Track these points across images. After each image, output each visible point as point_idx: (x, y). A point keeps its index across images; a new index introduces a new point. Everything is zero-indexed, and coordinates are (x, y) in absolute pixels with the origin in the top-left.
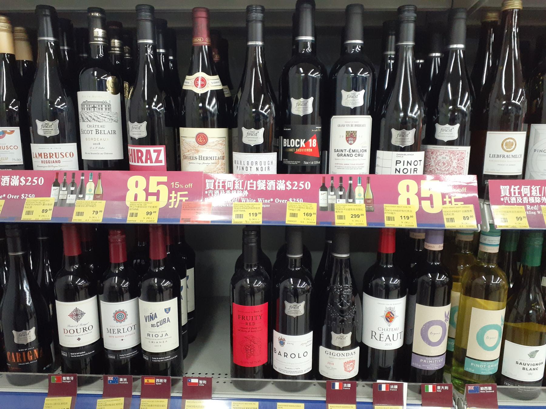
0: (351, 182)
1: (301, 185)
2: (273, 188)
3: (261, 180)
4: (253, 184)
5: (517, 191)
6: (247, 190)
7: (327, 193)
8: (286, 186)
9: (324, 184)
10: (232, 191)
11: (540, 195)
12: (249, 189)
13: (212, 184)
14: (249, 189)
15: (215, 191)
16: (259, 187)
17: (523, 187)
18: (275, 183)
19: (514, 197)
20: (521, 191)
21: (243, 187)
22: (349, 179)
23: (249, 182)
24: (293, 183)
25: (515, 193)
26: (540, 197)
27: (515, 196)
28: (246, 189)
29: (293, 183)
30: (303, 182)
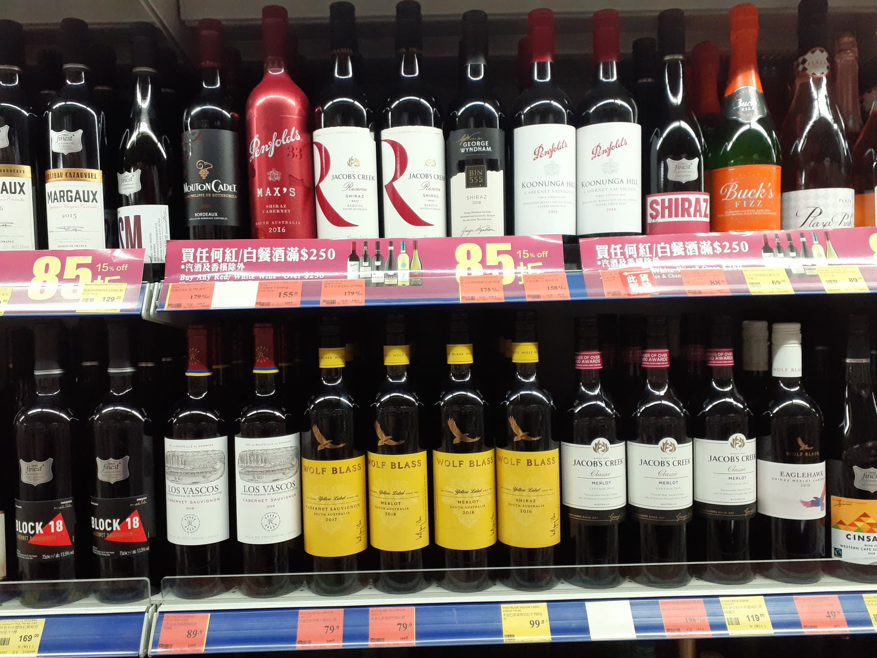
0: (392, 248)
1: (321, 253)
2: (281, 259)
3: (264, 248)
4: (252, 253)
5: (619, 251)
6: (243, 262)
7: (358, 265)
8: (301, 255)
9: (354, 252)
10: (221, 265)
11: (651, 256)
12: (245, 260)
13: (192, 255)
14: (245, 260)
15: (195, 264)
16: (261, 258)
17: (627, 245)
18: (283, 251)
19: (615, 259)
20: (625, 250)
21: (237, 258)
22: (389, 245)
23: (246, 251)
24: (311, 251)
25: (616, 254)
27: (616, 257)
28: (242, 260)
29: (311, 251)
30: (324, 250)
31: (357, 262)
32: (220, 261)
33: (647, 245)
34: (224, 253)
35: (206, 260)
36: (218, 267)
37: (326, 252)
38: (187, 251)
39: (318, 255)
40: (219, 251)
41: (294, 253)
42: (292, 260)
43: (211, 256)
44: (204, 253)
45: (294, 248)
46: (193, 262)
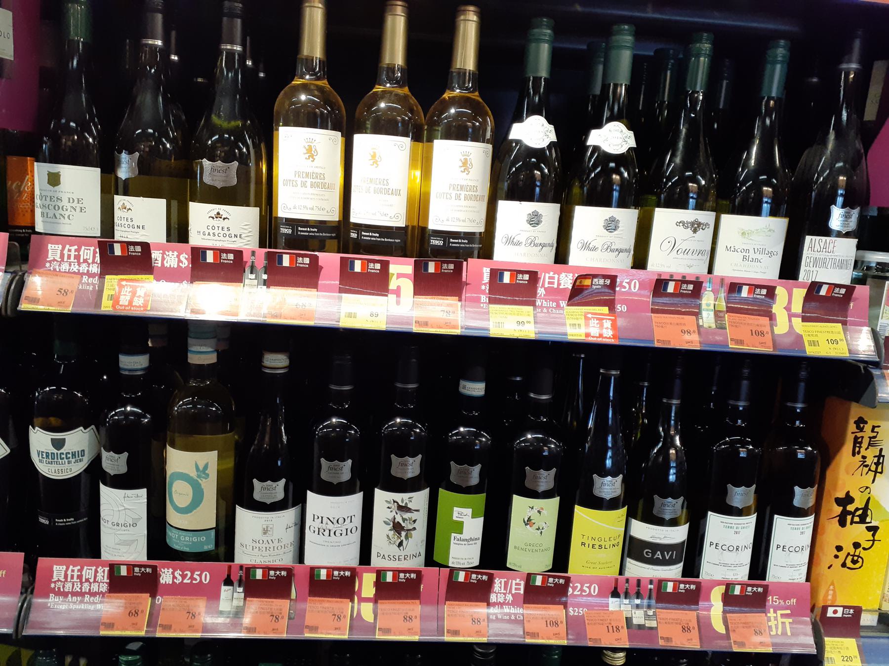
1: (195, 576)
7: (232, 589)
8: (174, 577)
9: (229, 576)
10: (92, 585)
11: (505, 592)
15: (66, 583)
24: (185, 573)
26: (505, 594)
29: (185, 573)
30: (198, 573)
31: (231, 587)
32: (92, 580)
33: (503, 580)
34: (96, 572)
35: (77, 579)
36: (89, 587)
37: (200, 576)
38: (58, 569)
39: (192, 578)
40: (91, 569)
41: (168, 575)
42: (166, 582)
43: (82, 575)
44: (76, 571)
45: (168, 569)
46: (63, 580)
